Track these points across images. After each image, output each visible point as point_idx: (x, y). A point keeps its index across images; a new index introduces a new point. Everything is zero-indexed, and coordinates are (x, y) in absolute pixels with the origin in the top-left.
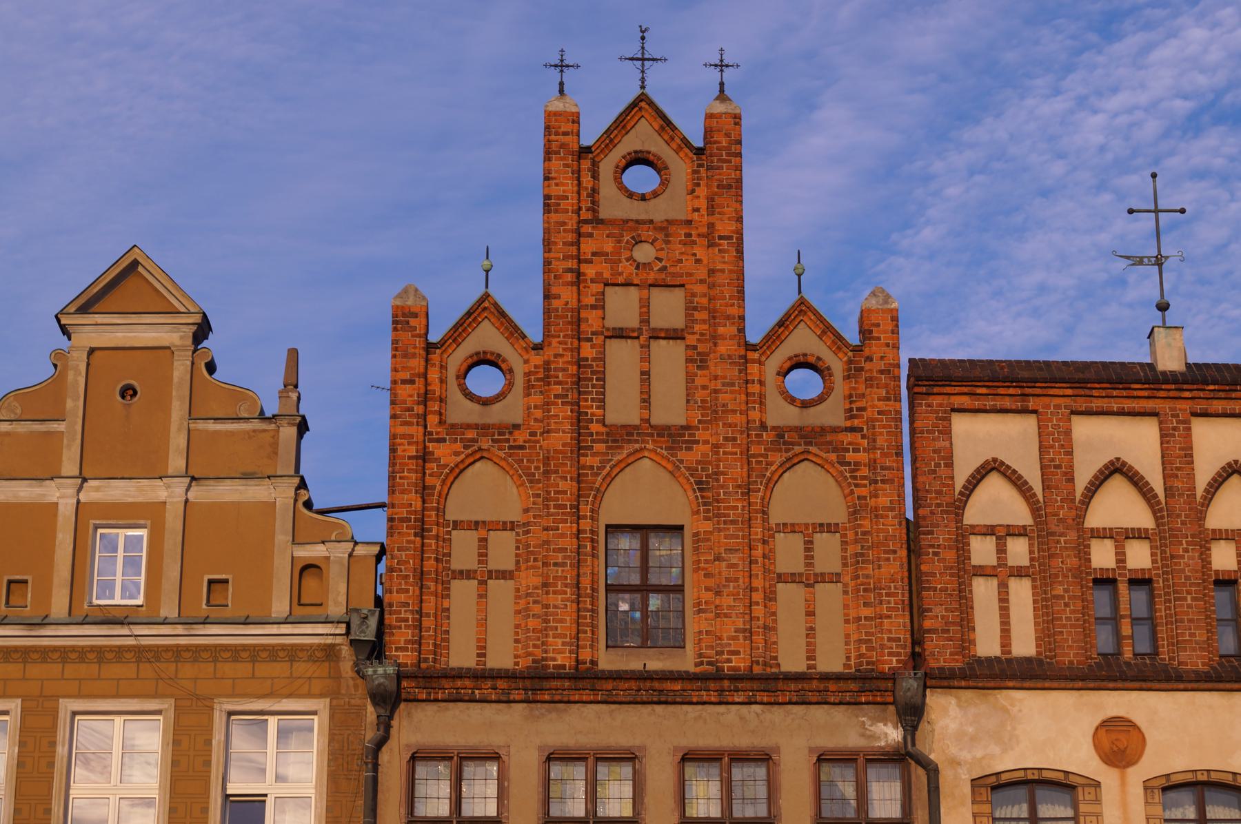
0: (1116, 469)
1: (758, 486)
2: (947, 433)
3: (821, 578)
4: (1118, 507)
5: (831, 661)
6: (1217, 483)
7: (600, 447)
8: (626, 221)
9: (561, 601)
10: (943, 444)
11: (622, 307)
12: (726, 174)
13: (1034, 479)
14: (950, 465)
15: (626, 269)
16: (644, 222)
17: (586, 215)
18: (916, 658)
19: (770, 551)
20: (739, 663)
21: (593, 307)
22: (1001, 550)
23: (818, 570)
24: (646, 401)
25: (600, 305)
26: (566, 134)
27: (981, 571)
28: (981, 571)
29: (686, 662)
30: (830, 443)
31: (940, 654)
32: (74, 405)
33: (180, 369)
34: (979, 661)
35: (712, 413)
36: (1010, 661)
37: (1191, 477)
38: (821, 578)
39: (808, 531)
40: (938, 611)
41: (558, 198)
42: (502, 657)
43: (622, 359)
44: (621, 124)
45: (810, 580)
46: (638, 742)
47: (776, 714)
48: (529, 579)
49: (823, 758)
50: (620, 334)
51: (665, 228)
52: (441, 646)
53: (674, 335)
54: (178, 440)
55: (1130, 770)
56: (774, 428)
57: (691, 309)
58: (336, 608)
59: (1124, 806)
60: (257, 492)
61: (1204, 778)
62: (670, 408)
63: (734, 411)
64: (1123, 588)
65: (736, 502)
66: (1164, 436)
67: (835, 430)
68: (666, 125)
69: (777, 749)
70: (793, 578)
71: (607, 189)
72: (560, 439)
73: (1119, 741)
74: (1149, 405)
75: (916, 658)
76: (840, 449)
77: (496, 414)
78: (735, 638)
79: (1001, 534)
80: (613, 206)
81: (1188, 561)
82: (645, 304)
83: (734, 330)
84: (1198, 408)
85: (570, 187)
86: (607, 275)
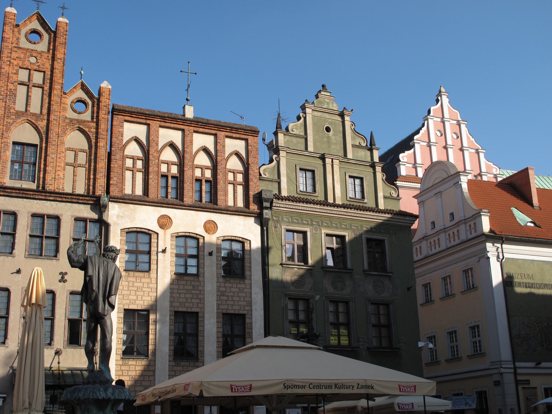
2: (122, 127)
3: (80, 166)
4: (169, 155)
5: (81, 189)
7: (13, 117)
8: (28, 49)
10: (121, 130)
11: (23, 75)
14: (122, 136)
15: (27, 64)
16: (34, 50)
17: (14, 45)
18: (108, 192)
19: (65, 155)
21: (15, 74)
23: (79, 163)
25: (17, 73)
26: (11, 19)
30: (86, 125)
31: (114, 191)
34: (126, 195)
36: (135, 196)
37: (192, 148)
38: (80, 166)
40: (115, 178)
41: (7, 38)
46: (17, 209)
50: (22, 84)
51: (41, 53)
55: (167, 230)
56: (69, 118)
59: (165, 240)
61: (187, 234)
63: (57, 112)
64: (170, 178)
67: (88, 122)
69: (62, 215)
73: (164, 222)
74: (182, 127)
78: (52, 180)
81: (188, 173)
83: (60, 87)
84: (196, 129)
86: (20, 64)
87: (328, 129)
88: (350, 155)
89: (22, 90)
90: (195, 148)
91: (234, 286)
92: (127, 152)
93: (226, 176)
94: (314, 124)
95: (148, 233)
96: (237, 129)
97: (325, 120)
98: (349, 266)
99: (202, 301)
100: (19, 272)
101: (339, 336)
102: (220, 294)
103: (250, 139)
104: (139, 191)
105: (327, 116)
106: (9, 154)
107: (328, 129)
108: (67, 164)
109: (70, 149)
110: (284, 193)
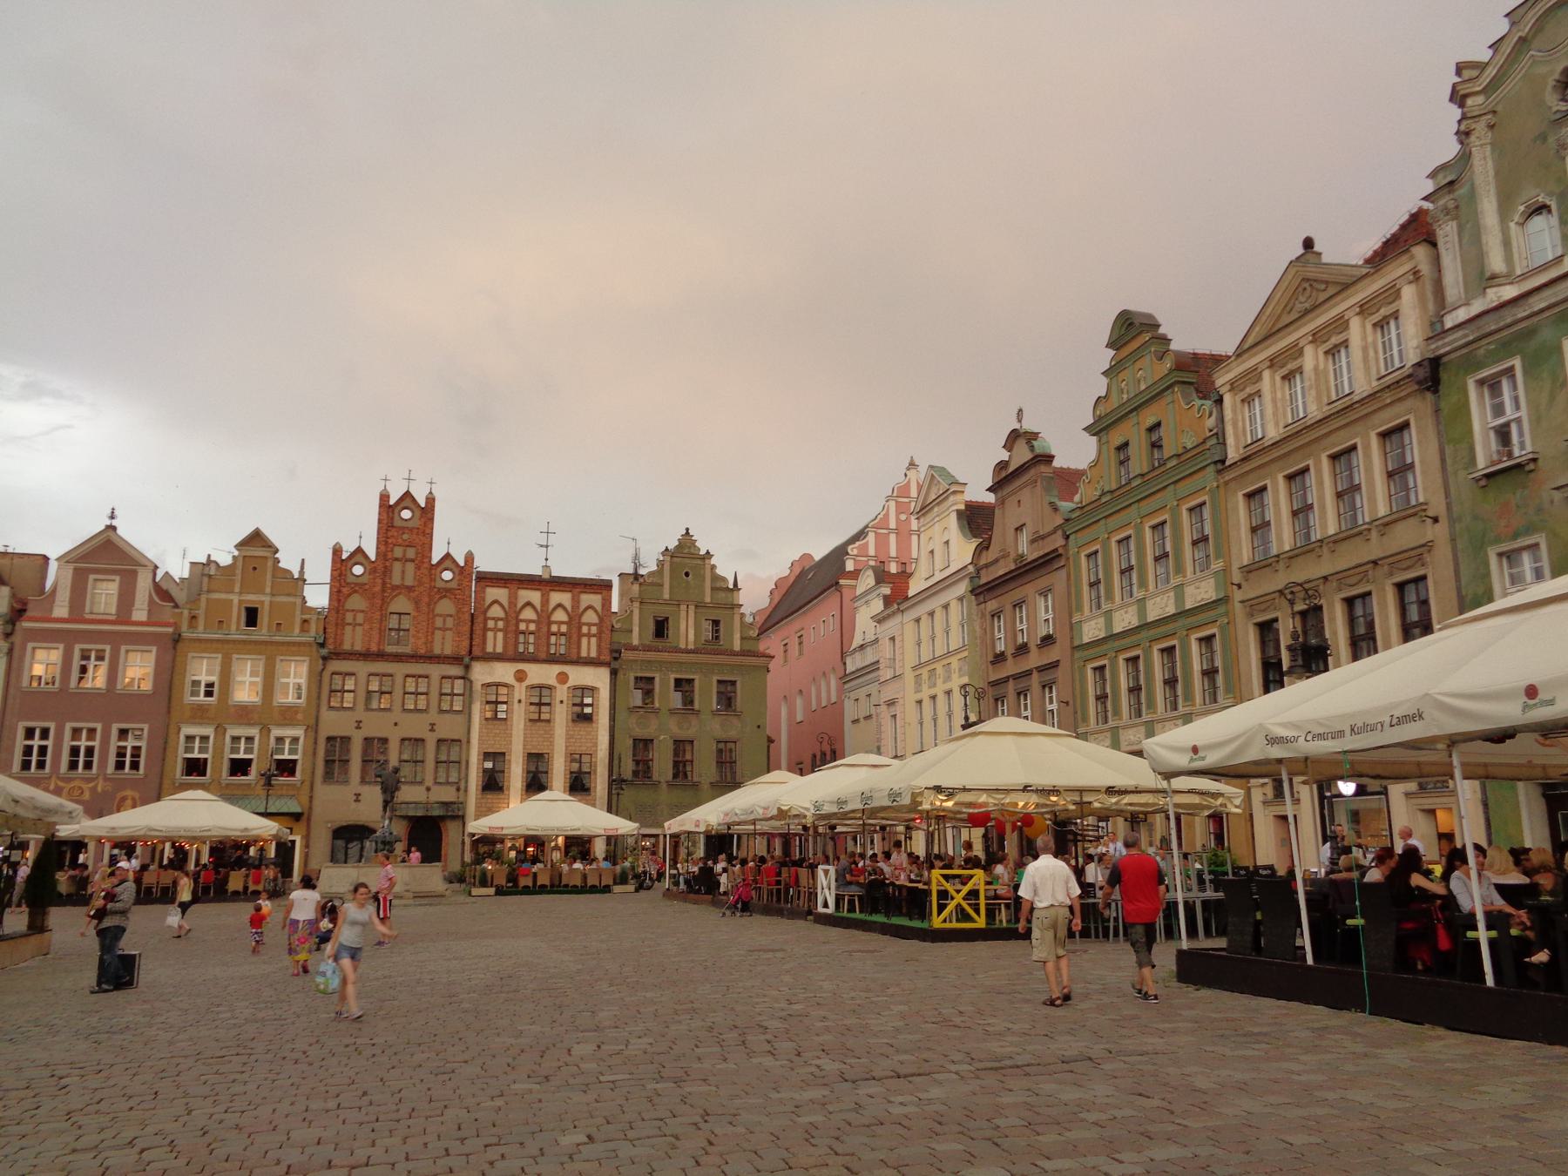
0: (528, 604)
1: (431, 604)
5: (448, 651)
9: (375, 633)
11: (398, 552)
13: (506, 604)
18: (470, 652)
20: (422, 652)
29: (407, 650)
31: (476, 651)
32: (239, 572)
33: (270, 563)
35: (420, 583)
42: (358, 647)
43: (397, 566)
44: (402, 499)
45: (444, 629)
48: (367, 627)
51: (411, 530)
52: (341, 644)
54: (269, 583)
58: (313, 633)
60: (291, 599)
62: (409, 581)
65: (425, 609)
68: (414, 500)
72: (378, 589)
73: (521, 676)
75: (470, 652)
77: (360, 580)
79: (496, 619)
80: (397, 523)
85: (385, 516)
87: (687, 574)
91: (583, 728)
92: (491, 613)
93: (580, 628)
98: (696, 706)
99: (552, 743)
102: (569, 737)
104: (499, 649)
107: (687, 574)
110: (636, 642)
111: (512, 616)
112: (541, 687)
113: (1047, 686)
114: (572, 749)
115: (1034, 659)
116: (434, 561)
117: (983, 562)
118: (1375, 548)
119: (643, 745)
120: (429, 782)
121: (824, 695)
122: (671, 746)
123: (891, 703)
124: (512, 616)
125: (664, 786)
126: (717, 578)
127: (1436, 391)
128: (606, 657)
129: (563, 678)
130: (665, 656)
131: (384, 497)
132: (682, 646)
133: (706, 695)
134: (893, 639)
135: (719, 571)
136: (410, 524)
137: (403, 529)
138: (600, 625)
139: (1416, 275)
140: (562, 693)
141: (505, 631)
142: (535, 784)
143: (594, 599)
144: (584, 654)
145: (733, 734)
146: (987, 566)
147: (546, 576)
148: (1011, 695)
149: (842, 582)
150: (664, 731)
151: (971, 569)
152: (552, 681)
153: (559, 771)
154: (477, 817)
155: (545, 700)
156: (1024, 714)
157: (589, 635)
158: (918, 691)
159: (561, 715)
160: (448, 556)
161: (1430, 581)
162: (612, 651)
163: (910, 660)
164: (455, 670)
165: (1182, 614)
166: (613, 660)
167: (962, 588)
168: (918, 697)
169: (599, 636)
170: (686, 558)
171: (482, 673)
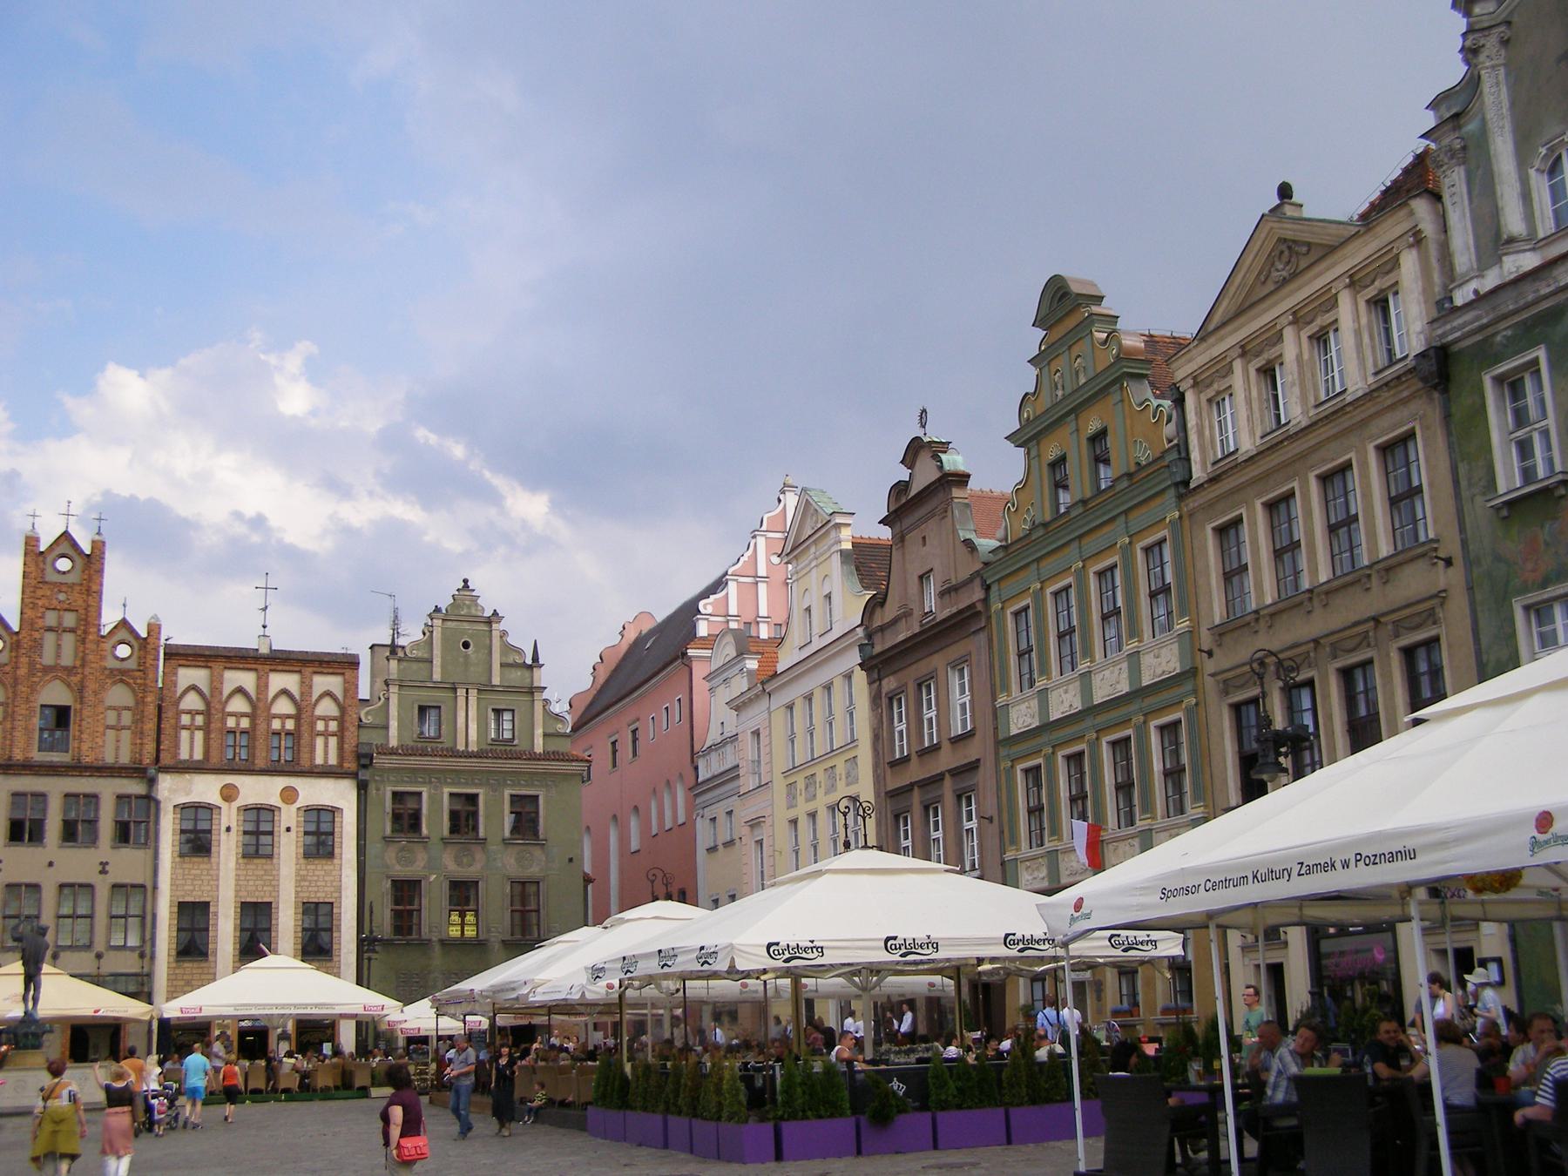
0: (240, 690)
2: (176, 674)
3: (123, 728)
4: (238, 705)
5: (125, 759)
6: (276, 697)
11: (51, 619)
12: (96, 567)
22: (193, 719)
24: (58, 655)
27: (184, 728)
28: (184, 728)
31: (166, 759)
35: (83, 666)
38: (123, 728)
39: (118, 710)
45: (118, 728)
47: (101, 780)
49: (119, 797)
50: (50, 629)
51: (72, 586)
53: (72, 630)
57: (79, 620)
62: (67, 659)
66: (259, 678)
68: (75, 545)
70: (112, 728)
71: (49, 570)
72: (22, 671)
73: (229, 794)
76: (134, 678)
81: (262, 727)
82: (60, 617)
87: (466, 645)
88: (496, 681)
89: (50, 638)
90: (272, 692)
91: (319, 868)
92: (184, 705)
93: (312, 725)
94: (445, 639)
95: (209, 808)
96: (328, 662)
97: (464, 632)
98: (482, 834)
99: (276, 888)
100: (51, 864)
101: (463, 925)
102: (300, 879)
103: (348, 673)
104: (198, 755)
105: (466, 626)
106: (37, 722)
107: (466, 645)
108: (109, 727)
109: (110, 708)
110: (393, 742)
111: (212, 708)
112: (259, 809)
113: (962, 796)
114: (305, 897)
115: (947, 760)
116: (105, 631)
117: (877, 623)
118: (1374, 601)
119: (406, 890)
120: (99, 946)
121: (668, 814)
122: (446, 885)
123: (755, 824)
124: (212, 708)
125: (437, 947)
126: (508, 648)
127: (1445, 391)
128: (350, 765)
129: (289, 795)
130: (437, 762)
131: (31, 542)
132: (461, 747)
133: (496, 818)
134: (757, 733)
135: (511, 640)
136: (70, 579)
137: (59, 586)
138: (341, 720)
139: (1418, 239)
140: (289, 816)
141: (206, 729)
142: (253, 946)
143: (333, 683)
144: (319, 760)
145: (534, 871)
146: (882, 629)
147: (264, 650)
148: (917, 808)
149: (691, 652)
150: (436, 864)
151: (860, 631)
152: (275, 800)
153: (287, 923)
154: (171, 996)
155: (264, 827)
156: (905, 843)
157: (326, 734)
158: (791, 806)
159: (289, 847)
160: (124, 623)
161: (1376, 664)
162: (359, 756)
163: (781, 763)
164: (135, 787)
165: (1090, 710)
166: (359, 766)
167: (854, 658)
168: (792, 814)
169: (341, 734)
170: (465, 621)
171: (172, 791)
